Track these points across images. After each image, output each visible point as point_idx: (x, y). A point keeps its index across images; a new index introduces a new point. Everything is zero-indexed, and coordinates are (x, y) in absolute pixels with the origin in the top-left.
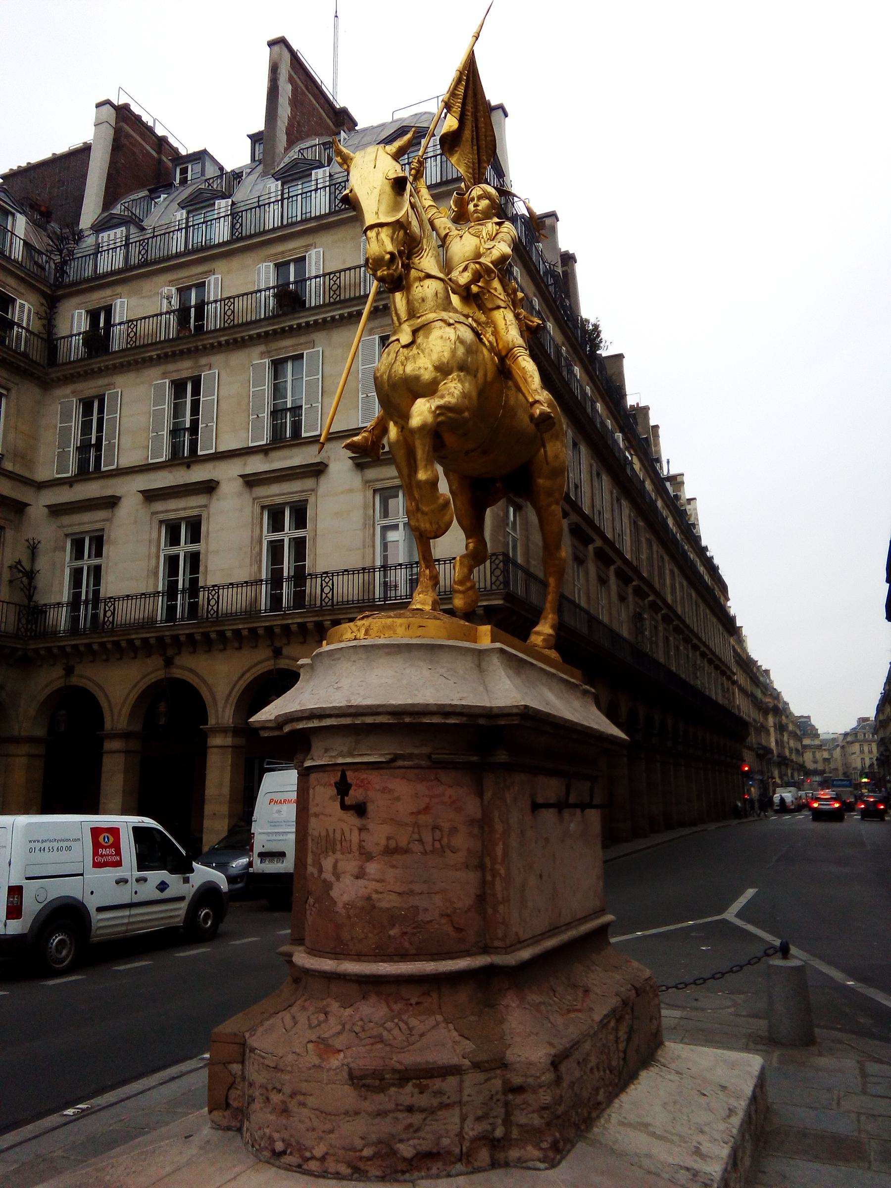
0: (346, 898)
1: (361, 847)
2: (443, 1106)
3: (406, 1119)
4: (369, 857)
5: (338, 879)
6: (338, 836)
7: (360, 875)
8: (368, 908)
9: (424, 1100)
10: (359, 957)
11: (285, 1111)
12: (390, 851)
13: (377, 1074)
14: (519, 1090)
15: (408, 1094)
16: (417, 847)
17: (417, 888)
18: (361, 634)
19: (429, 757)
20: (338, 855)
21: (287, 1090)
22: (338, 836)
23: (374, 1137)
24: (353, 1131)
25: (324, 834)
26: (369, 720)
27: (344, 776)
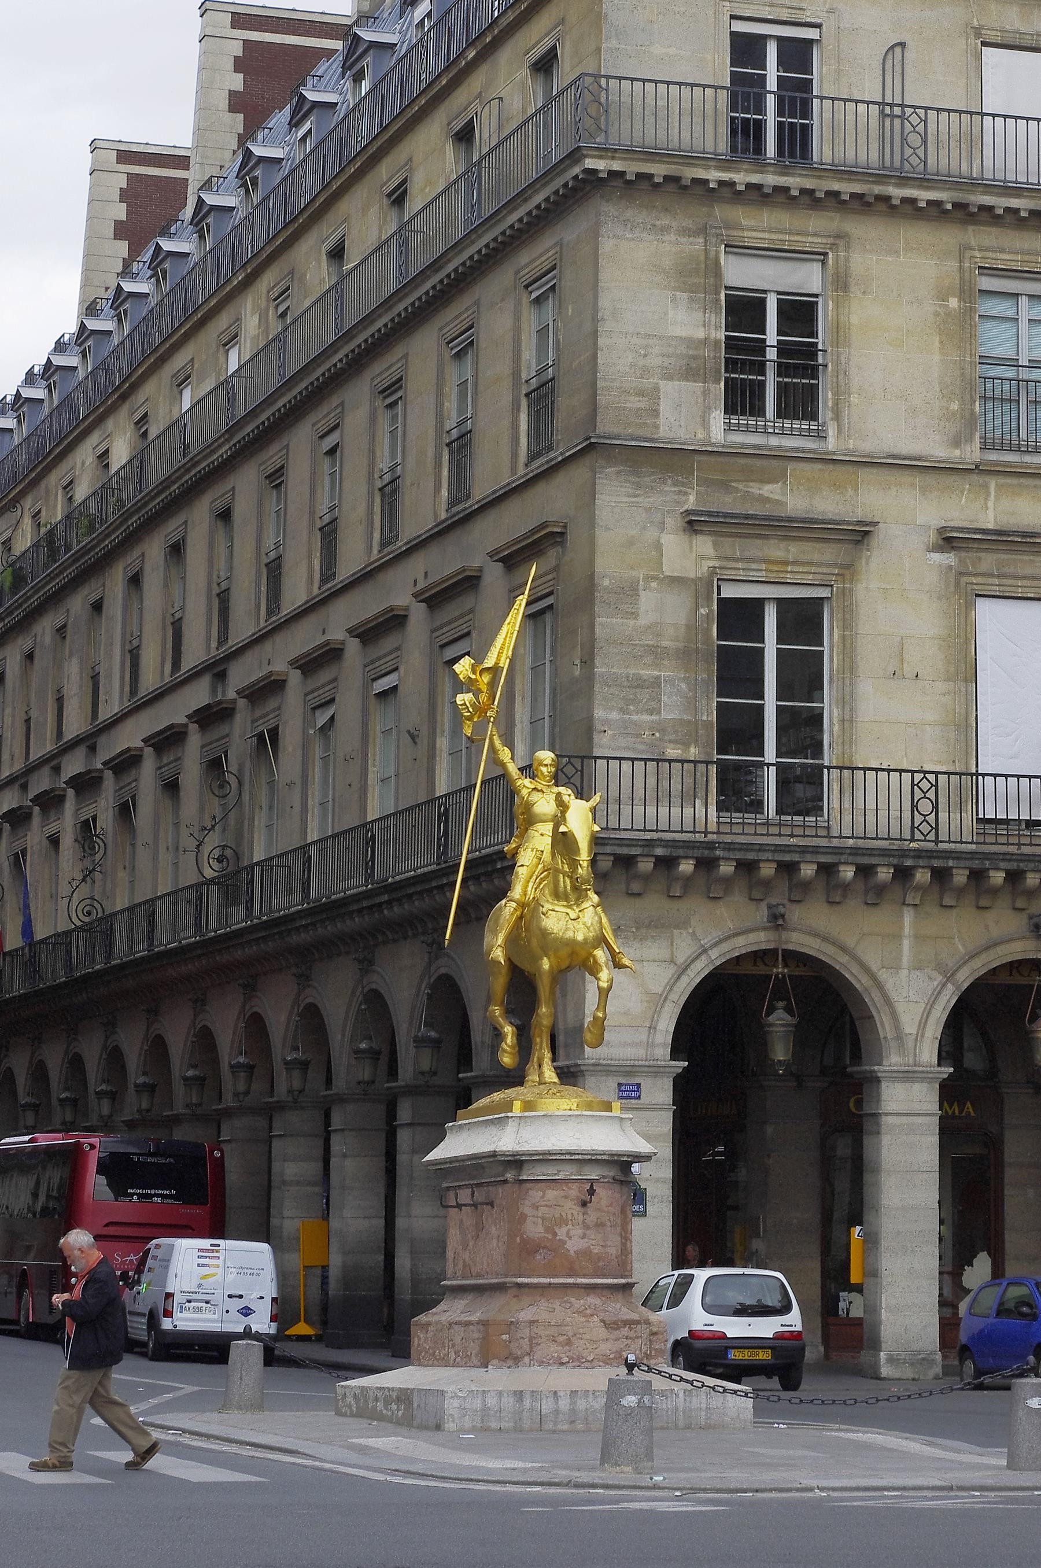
0: (575, 1249)
1: (584, 1222)
2: (637, 1337)
3: (626, 1342)
4: (588, 1228)
5: (570, 1238)
6: (570, 1217)
7: (584, 1237)
8: (586, 1253)
9: (632, 1334)
10: (584, 1276)
11: (569, 1343)
12: (600, 1225)
13: (615, 1323)
14: (655, 1334)
15: (625, 1331)
16: (609, 1224)
17: (609, 1243)
18: (574, 1107)
19: (614, 1178)
20: (570, 1226)
21: (570, 1334)
22: (570, 1217)
23: (614, 1350)
24: (605, 1348)
25: (557, 1216)
26: (599, 1157)
27: (592, 1186)
